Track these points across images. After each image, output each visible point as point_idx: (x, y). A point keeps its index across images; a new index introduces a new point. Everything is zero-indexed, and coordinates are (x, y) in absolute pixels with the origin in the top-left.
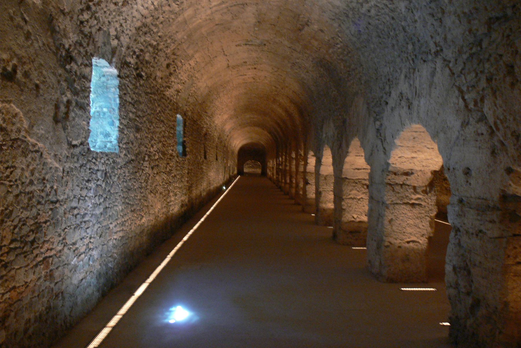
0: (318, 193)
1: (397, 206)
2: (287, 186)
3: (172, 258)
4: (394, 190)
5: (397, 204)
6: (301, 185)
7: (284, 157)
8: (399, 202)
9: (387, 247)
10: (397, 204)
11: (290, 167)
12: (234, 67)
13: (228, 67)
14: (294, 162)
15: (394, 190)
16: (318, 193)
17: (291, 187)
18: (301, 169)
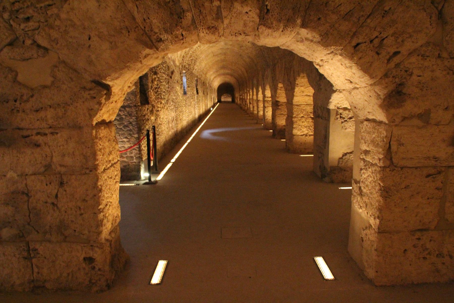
0: (253, 107)
1: (269, 107)
2: (244, 106)
3: (183, 151)
4: (267, 102)
5: (269, 106)
6: (249, 105)
7: (242, 92)
8: (269, 106)
9: (266, 119)
10: (269, 106)
11: (245, 97)
12: (216, 56)
13: (214, 55)
14: (246, 95)
15: (267, 102)
16: (253, 107)
17: (245, 106)
18: (248, 98)
